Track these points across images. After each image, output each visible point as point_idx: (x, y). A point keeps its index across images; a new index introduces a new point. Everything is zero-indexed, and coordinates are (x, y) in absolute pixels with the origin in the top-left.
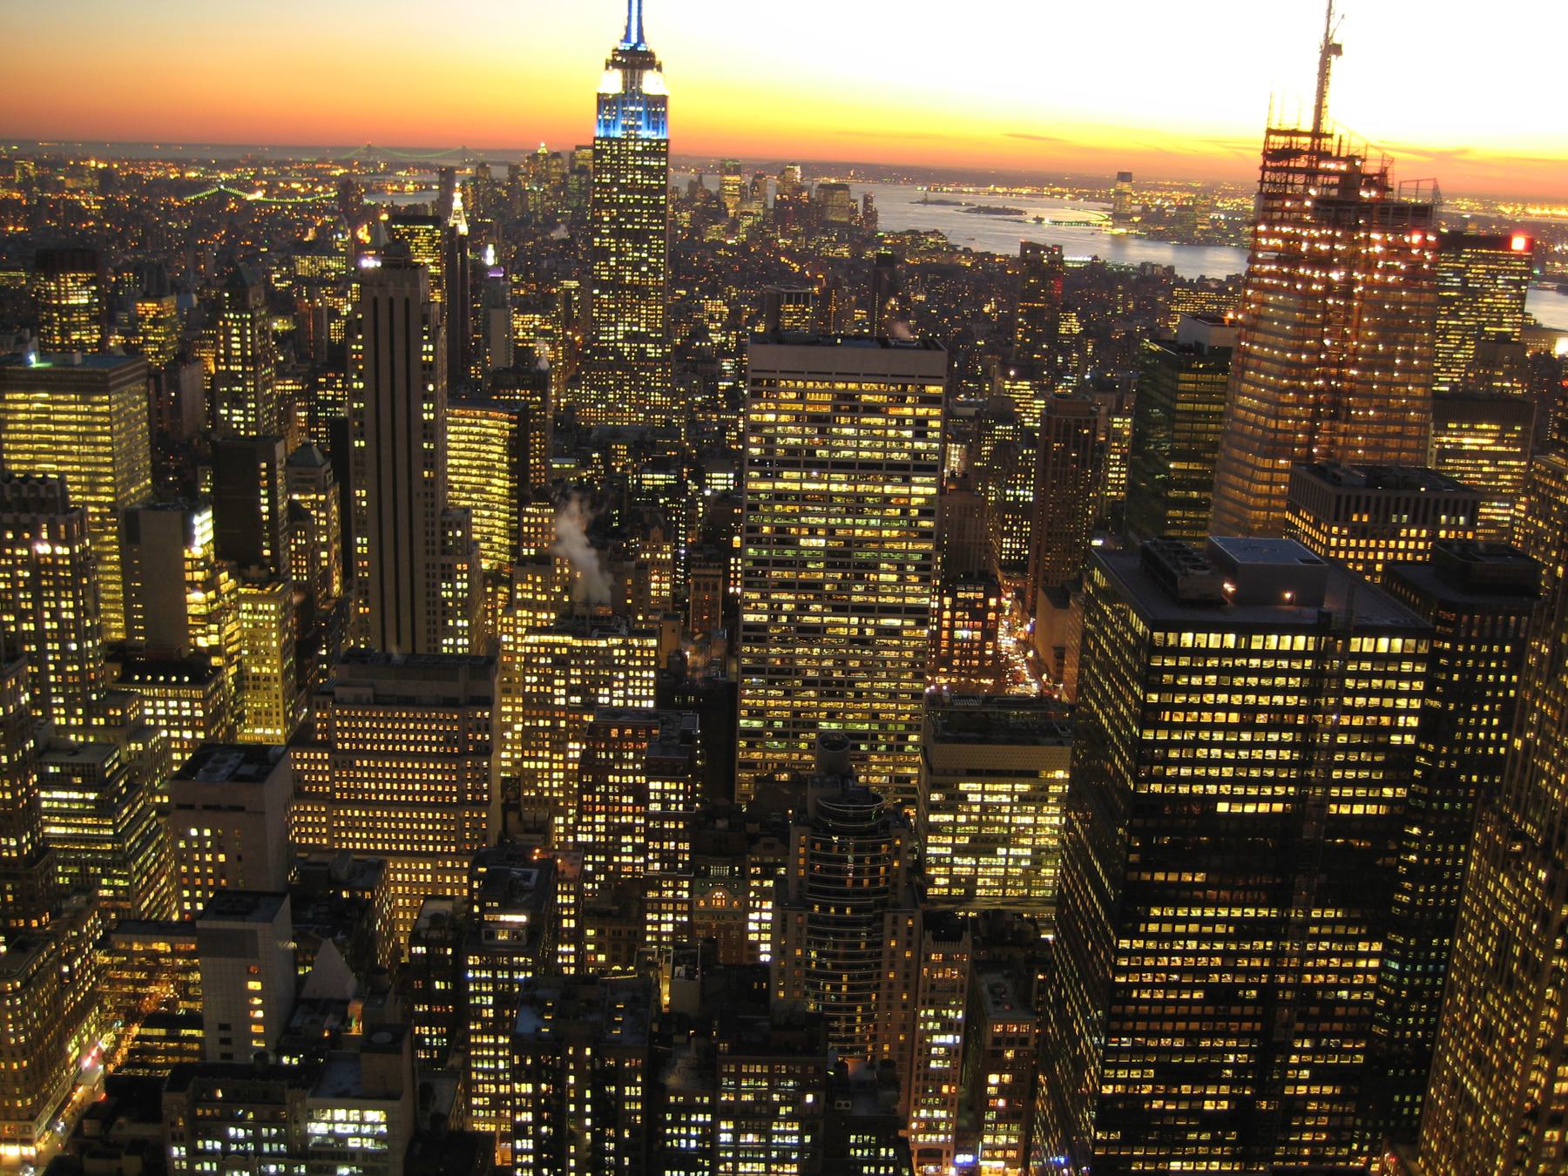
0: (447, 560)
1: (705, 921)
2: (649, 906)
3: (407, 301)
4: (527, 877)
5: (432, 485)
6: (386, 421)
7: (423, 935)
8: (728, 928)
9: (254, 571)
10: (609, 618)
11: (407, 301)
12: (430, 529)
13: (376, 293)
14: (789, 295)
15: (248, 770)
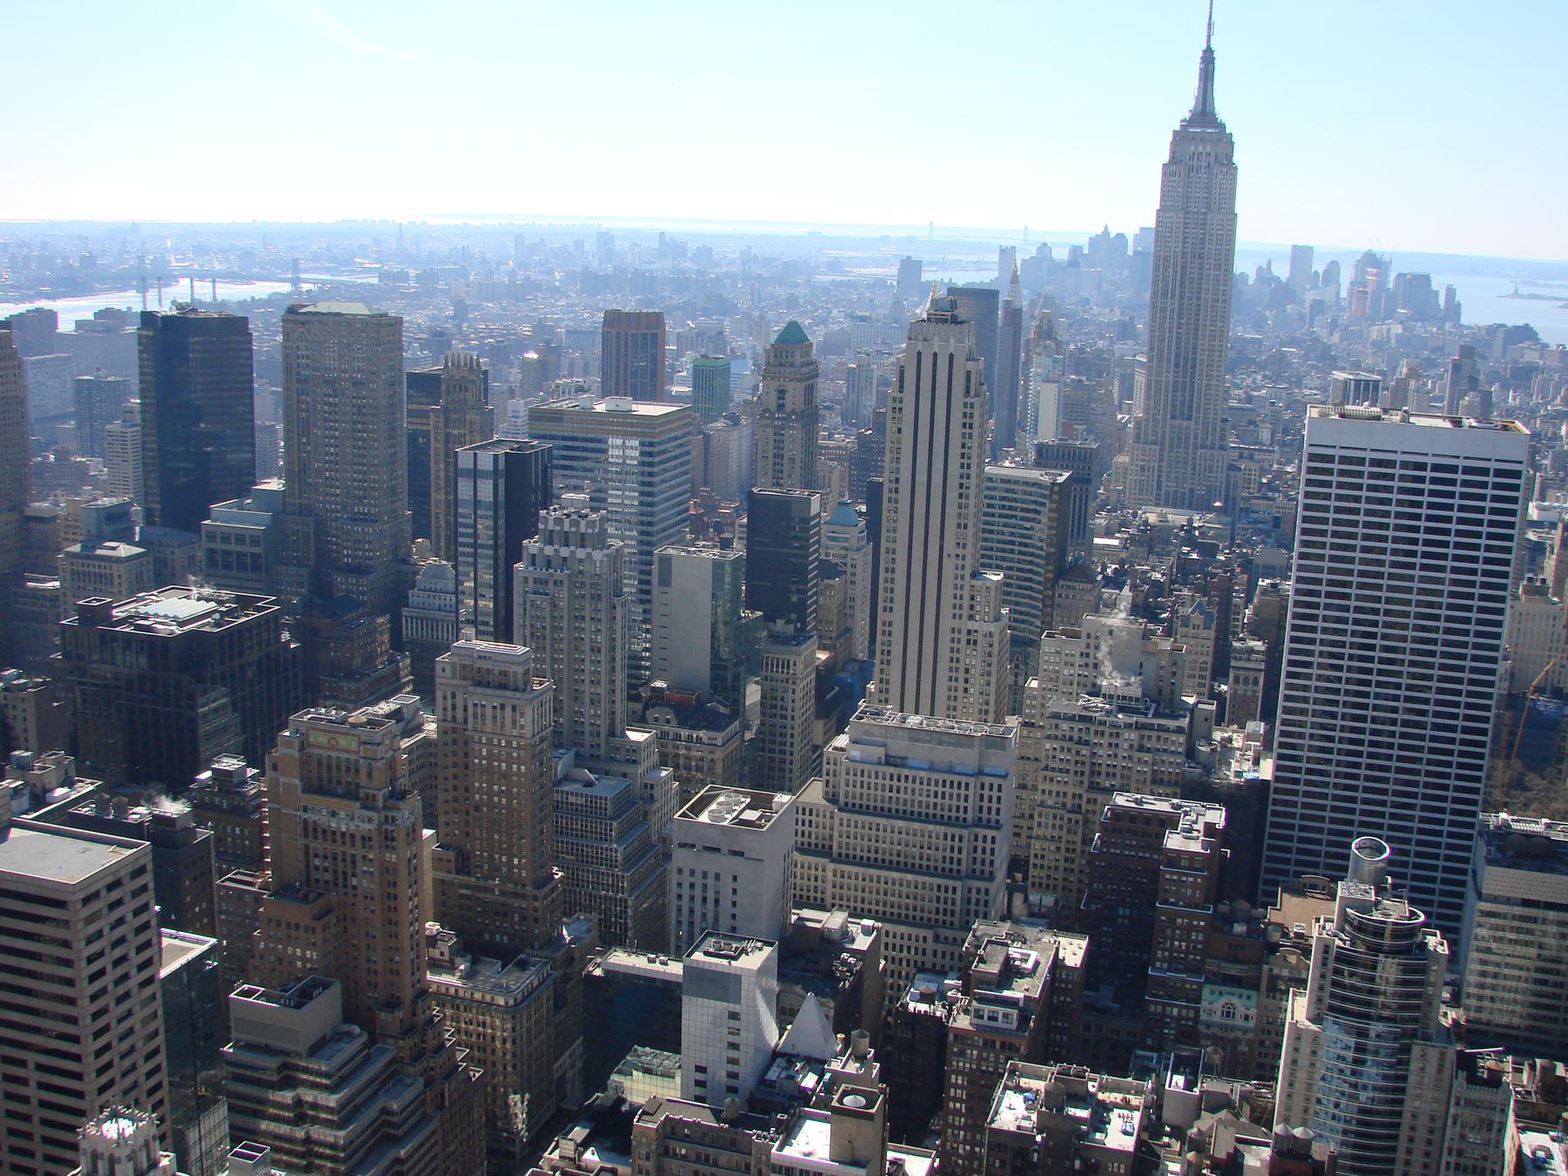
0: (972, 625)
1: (1212, 1030)
2: (1152, 1008)
3: (951, 356)
4: (1025, 960)
5: (964, 547)
6: (922, 478)
7: (911, 1006)
8: (1237, 1041)
9: (780, 625)
10: (1137, 700)
11: (951, 356)
12: (958, 592)
13: (920, 348)
14: (1358, 382)
15: (751, 815)
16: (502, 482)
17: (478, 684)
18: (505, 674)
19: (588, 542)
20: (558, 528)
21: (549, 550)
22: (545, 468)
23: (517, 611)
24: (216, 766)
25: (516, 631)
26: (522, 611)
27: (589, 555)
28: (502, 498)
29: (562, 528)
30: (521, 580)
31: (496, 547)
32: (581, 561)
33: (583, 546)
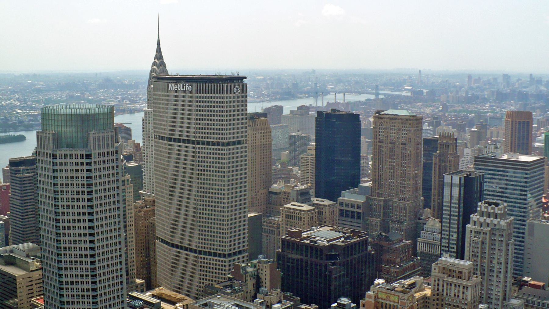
16: (462, 188)
17: (449, 276)
18: (460, 272)
19: (498, 217)
20: (486, 210)
21: (482, 220)
22: (481, 183)
23: (467, 244)
24: (339, 301)
25: (466, 254)
26: (469, 245)
27: (499, 222)
28: (462, 196)
29: (488, 210)
30: (470, 232)
31: (459, 216)
32: (495, 225)
33: (496, 218)
